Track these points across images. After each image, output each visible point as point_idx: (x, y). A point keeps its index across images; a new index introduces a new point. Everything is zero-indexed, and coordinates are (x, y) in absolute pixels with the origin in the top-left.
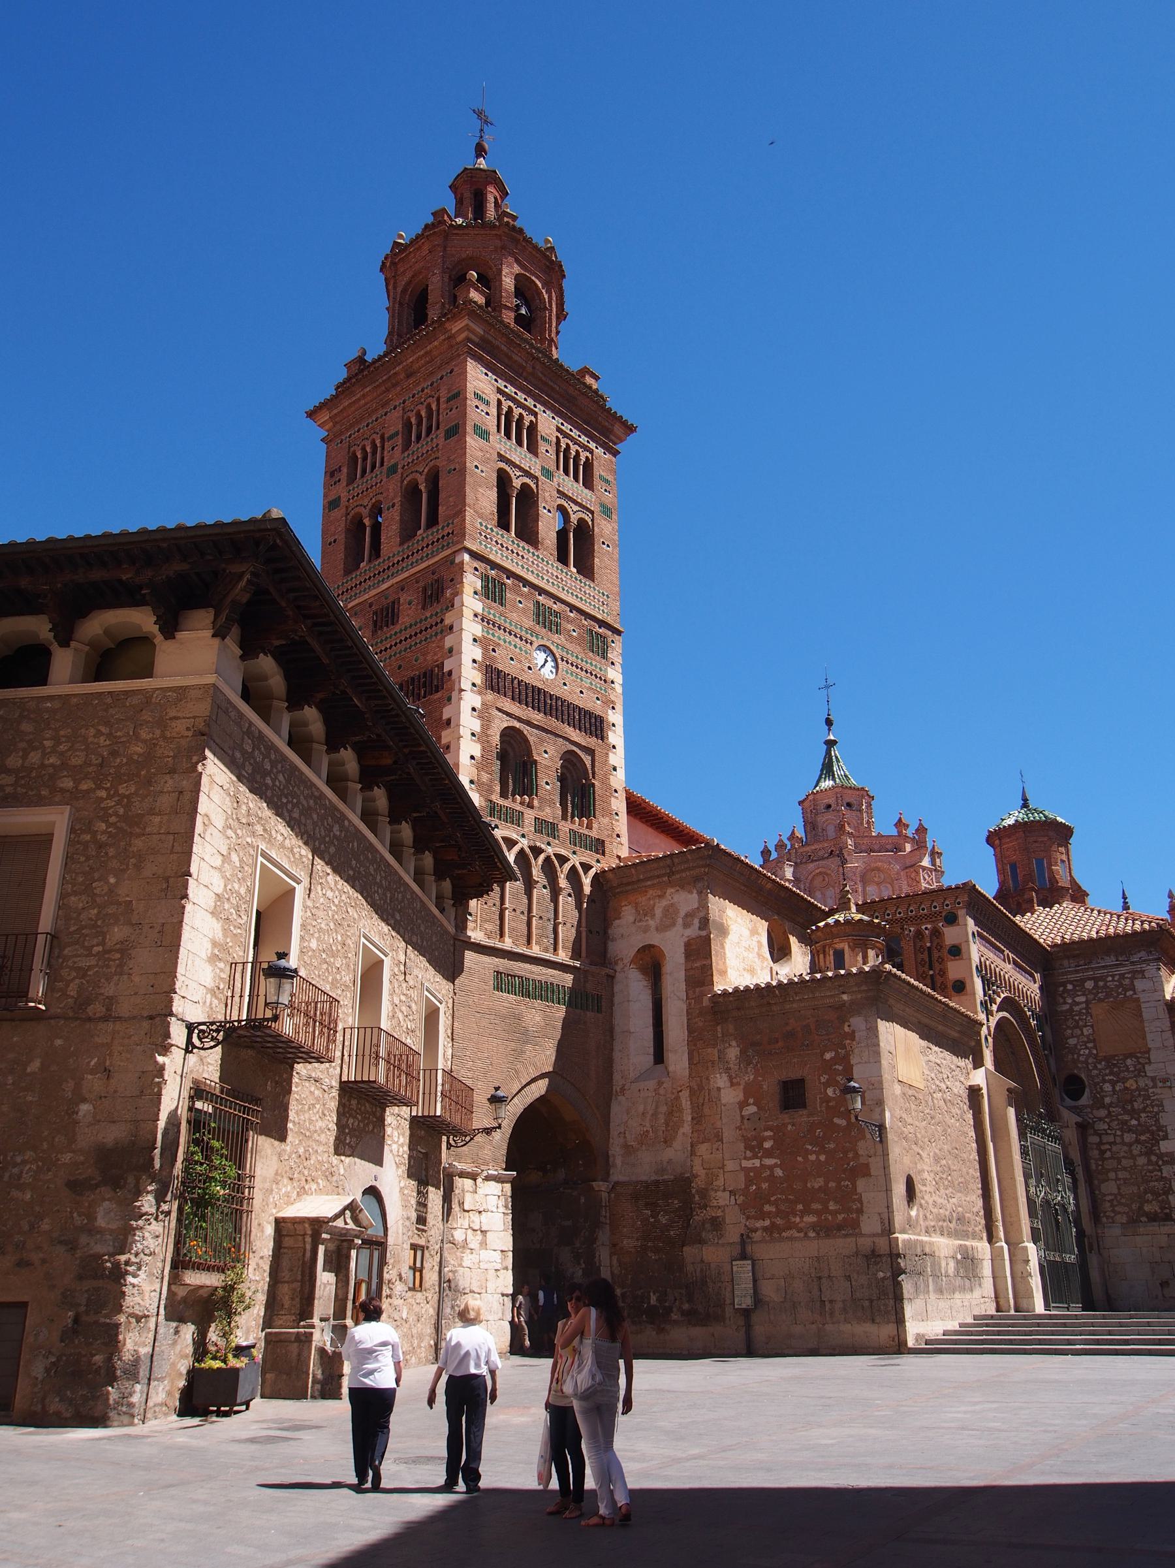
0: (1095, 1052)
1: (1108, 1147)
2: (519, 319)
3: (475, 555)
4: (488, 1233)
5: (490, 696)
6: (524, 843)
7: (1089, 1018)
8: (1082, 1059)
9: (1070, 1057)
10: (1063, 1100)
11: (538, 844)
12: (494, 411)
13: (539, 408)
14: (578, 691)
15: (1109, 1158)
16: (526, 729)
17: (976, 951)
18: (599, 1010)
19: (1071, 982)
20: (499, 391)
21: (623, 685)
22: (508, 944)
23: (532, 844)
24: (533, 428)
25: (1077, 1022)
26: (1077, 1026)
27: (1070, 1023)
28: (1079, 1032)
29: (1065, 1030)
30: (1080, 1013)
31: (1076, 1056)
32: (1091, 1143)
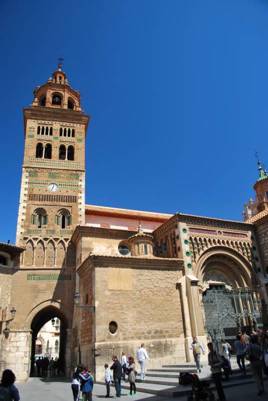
2: (54, 103)
3: (26, 167)
4: (20, 348)
5: (30, 202)
6: (41, 238)
11: (47, 237)
12: (36, 130)
13: (55, 122)
14: (66, 191)
16: (44, 207)
17: (184, 236)
18: (70, 279)
20: (39, 124)
21: (85, 185)
22: (34, 267)
23: (44, 237)
24: (51, 128)
27: (265, 248)
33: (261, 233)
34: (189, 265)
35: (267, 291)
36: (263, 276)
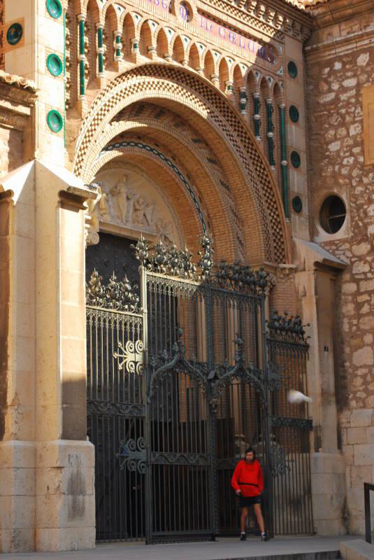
0: (361, 159)
1: (366, 297)
7: (359, 110)
8: (344, 171)
9: (330, 169)
10: (313, 234)
15: (368, 314)
19: (340, 59)
25: (343, 117)
26: (343, 124)
27: (334, 120)
28: (344, 132)
29: (327, 131)
30: (348, 104)
31: (337, 167)
32: (345, 294)
33: (329, 55)
34: (55, 116)
35: (316, 294)
36: (306, 233)
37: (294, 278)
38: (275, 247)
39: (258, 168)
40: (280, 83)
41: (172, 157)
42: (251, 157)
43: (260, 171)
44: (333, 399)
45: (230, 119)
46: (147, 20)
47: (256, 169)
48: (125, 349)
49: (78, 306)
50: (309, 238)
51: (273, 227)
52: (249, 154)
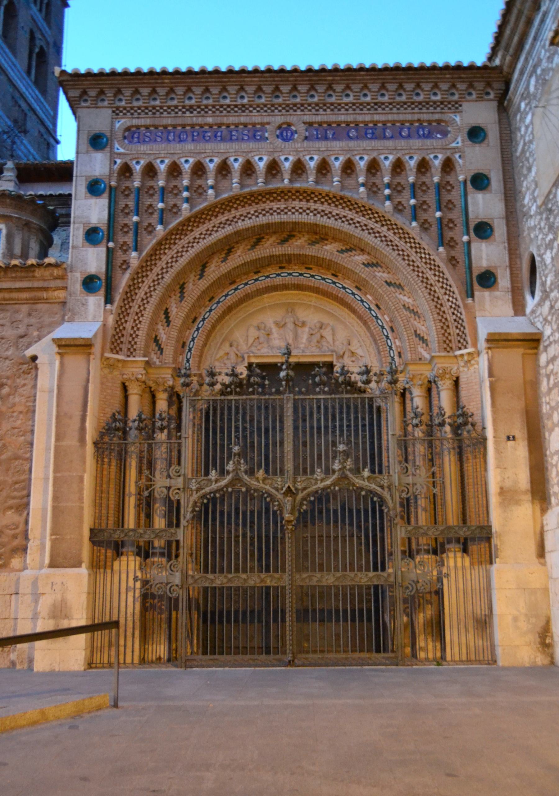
26: (529, 169)
35: (491, 375)
36: (508, 309)
37: (478, 364)
38: (458, 335)
39: (423, 255)
40: (457, 156)
41: (333, 275)
42: (411, 247)
43: (425, 258)
44: (529, 497)
45: (371, 216)
46: (227, 158)
47: (421, 258)
48: (154, 476)
49: (78, 444)
50: (512, 312)
51: (453, 314)
52: (409, 245)
